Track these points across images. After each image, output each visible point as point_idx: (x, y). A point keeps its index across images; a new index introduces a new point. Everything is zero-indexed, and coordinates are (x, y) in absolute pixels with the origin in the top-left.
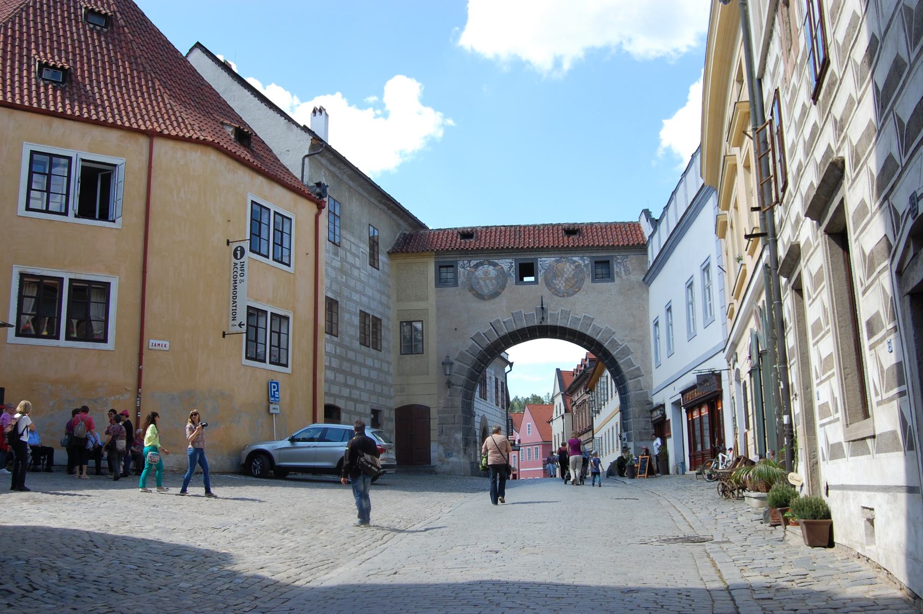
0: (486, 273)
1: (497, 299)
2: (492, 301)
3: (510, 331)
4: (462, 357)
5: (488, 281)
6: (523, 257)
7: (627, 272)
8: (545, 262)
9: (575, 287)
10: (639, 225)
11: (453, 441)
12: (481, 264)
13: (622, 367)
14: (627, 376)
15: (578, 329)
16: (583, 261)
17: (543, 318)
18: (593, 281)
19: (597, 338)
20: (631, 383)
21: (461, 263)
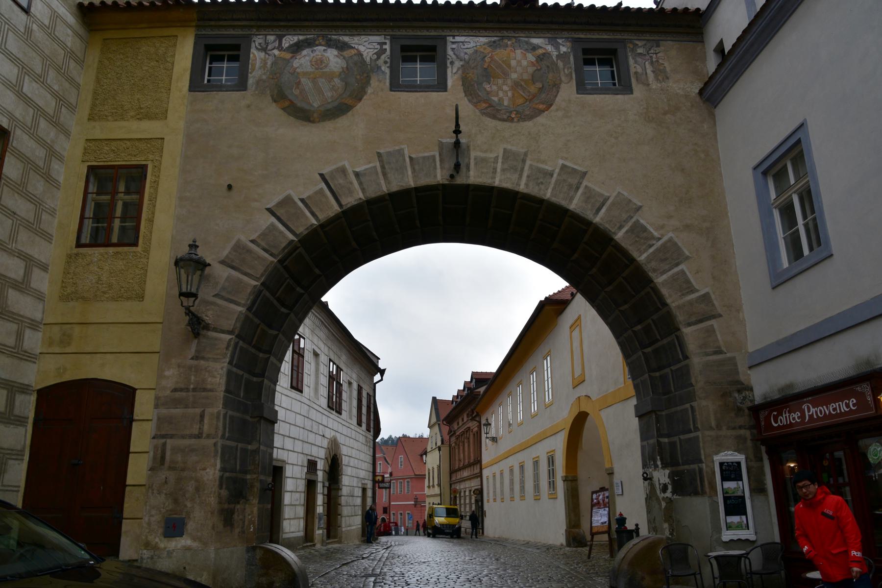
0: (320, 63)
1: (343, 121)
2: (329, 125)
3: (372, 193)
5: (322, 82)
7: (661, 74)
8: (464, 45)
9: (536, 99)
11: (190, 488)
12: (309, 44)
13: (664, 291)
14: (680, 317)
15: (548, 194)
17: (457, 167)
19: (597, 220)
21: (258, 40)
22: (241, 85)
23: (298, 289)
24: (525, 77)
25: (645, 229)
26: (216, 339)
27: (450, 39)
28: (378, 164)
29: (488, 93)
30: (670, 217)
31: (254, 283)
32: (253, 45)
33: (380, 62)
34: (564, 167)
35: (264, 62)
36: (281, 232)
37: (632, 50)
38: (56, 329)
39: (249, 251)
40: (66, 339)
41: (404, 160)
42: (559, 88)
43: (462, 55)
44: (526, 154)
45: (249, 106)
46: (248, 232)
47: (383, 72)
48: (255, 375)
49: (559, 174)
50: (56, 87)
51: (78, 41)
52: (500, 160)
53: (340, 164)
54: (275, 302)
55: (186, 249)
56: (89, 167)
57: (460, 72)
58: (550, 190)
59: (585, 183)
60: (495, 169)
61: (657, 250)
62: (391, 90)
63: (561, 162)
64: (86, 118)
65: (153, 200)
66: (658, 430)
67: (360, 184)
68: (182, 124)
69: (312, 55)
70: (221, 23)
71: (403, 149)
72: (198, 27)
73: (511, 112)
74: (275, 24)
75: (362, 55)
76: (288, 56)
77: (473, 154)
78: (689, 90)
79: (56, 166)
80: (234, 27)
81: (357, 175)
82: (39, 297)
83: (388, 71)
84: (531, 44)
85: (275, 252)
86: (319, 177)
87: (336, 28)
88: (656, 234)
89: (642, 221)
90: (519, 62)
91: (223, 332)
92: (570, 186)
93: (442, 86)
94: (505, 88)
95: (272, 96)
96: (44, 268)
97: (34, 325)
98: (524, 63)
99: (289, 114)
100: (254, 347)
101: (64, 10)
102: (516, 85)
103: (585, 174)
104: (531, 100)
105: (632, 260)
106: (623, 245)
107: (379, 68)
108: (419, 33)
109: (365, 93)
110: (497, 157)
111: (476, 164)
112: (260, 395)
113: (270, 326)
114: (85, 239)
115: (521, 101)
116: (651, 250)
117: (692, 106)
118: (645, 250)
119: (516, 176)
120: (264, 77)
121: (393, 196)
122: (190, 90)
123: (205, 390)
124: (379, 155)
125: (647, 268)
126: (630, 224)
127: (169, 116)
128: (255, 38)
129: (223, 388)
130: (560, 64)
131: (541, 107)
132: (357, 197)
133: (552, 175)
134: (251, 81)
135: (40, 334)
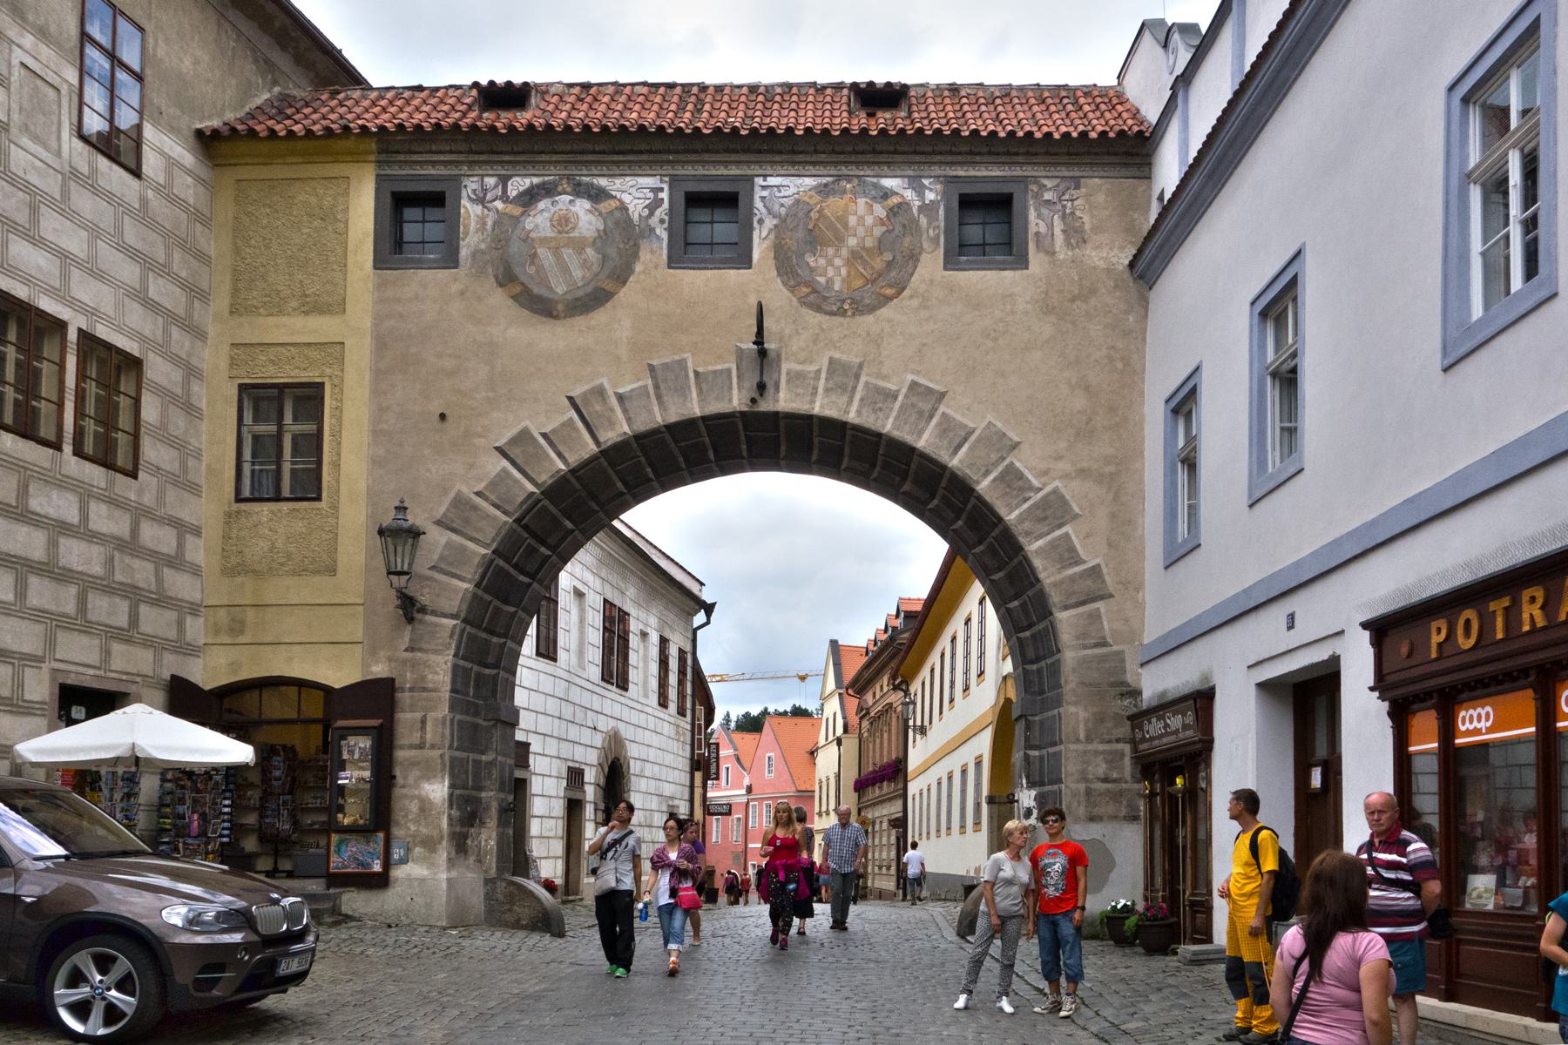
0: (564, 222)
1: (599, 317)
2: (580, 321)
4: (458, 518)
5: (567, 253)
6: (700, 171)
8: (780, 190)
10: (1120, 95)
12: (547, 191)
15: (887, 426)
16: (919, 192)
17: (761, 387)
18: (950, 263)
19: (954, 463)
20: (1066, 621)
21: (471, 185)
22: (450, 260)
23: (543, 549)
24: (869, 243)
25: (1021, 476)
26: (436, 625)
27: (759, 181)
28: (649, 382)
29: (812, 270)
30: (1059, 458)
31: (483, 551)
32: (464, 193)
33: (654, 221)
34: (914, 385)
35: (482, 221)
36: (516, 481)
37: (1037, 196)
38: (222, 613)
39: (475, 508)
40: (237, 627)
41: (687, 376)
42: (918, 260)
43: (776, 207)
44: (861, 366)
45: (462, 293)
46: (475, 481)
47: (658, 237)
48: (487, 666)
49: (906, 396)
50: (184, 274)
51: (201, 189)
52: (823, 375)
53: (597, 382)
54: (512, 571)
55: (392, 513)
56: (240, 386)
57: (772, 237)
58: (891, 420)
59: (942, 409)
60: (815, 389)
61: (1034, 505)
62: (670, 267)
63: (910, 377)
64: (227, 310)
65: (337, 434)
66: (1027, 739)
67: (625, 411)
68: (368, 323)
69: (553, 210)
70: (415, 157)
71: (685, 360)
72: (379, 163)
73: (843, 301)
74: (495, 158)
75: (627, 209)
76: (517, 211)
77: (785, 366)
78: (1115, 260)
79: (195, 387)
80: (434, 163)
81: (621, 398)
82: (196, 571)
83: (665, 236)
84: (882, 188)
85: (509, 508)
86: (566, 402)
87: (587, 163)
88: (1036, 483)
89: (1018, 464)
90: (861, 218)
91: (445, 616)
92: (921, 413)
93: (745, 261)
94: (838, 262)
95: (496, 277)
96: (197, 532)
97: (194, 609)
98: (869, 220)
99: (522, 305)
100: (485, 630)
101: (179, 149)
102: (855, 256)
103: (943, 395)
104: (874, 281)
105: (1000, 519)
106: (987, 498)
107: (652, 230)
108: (714, 172)
109: (632, 272)
110: (819, 371)
111: (788, 382)
112: (494, 692)
113: (506, 602)
114: (246, 493)
115: (859, 283)
116: (1026, 506)
117: (1116, 286)
118: (1018, 506)
119: (845, 398)
120: (483, 246)
121: (673, 429)
122: (375, 268)
123: (425, 689)
124: (652, 368)
125: (1017, 530)
126: (1000, 468)
127: (348, 306)
128: (466, 182)
129: (448, 687)
130: (923, 221)
131: (889, 291)
132: (621, 431)
133: (896, 398)
134: (464, 252)
135: (202, 620)
